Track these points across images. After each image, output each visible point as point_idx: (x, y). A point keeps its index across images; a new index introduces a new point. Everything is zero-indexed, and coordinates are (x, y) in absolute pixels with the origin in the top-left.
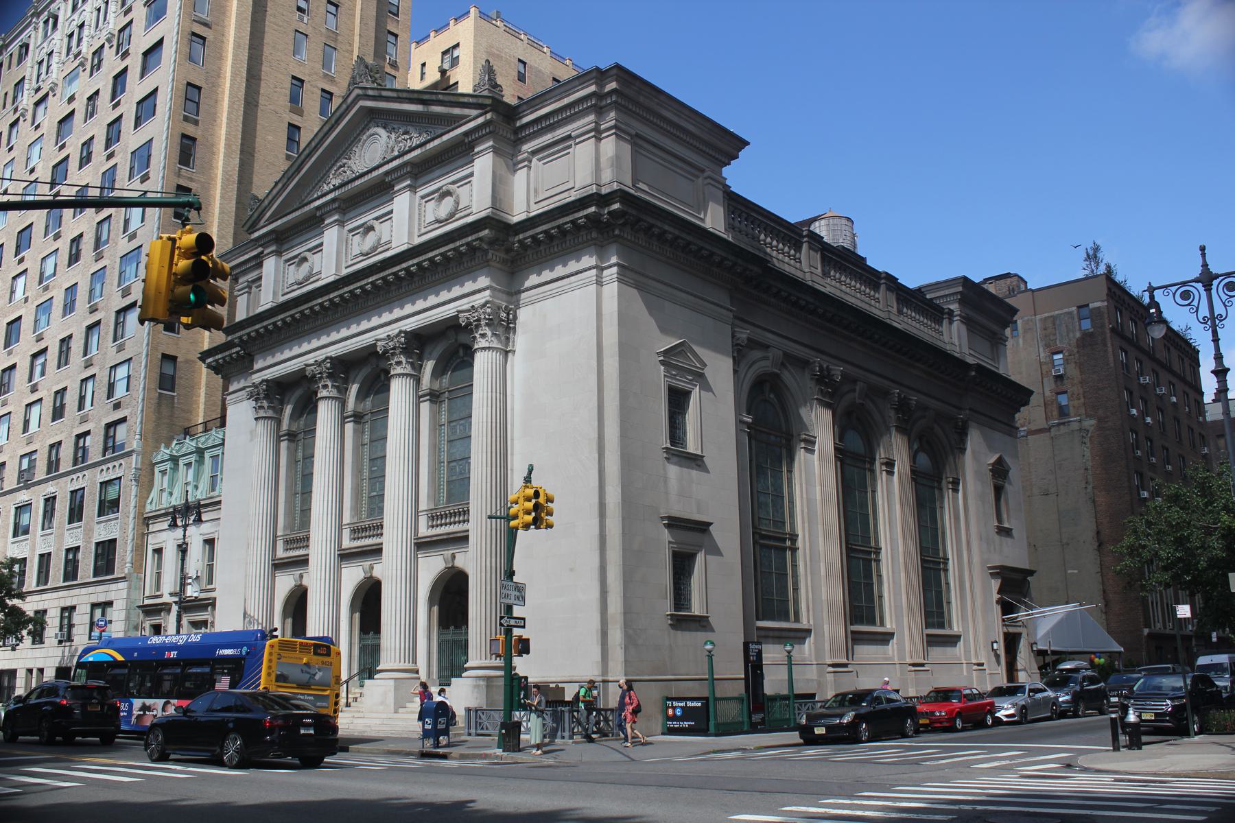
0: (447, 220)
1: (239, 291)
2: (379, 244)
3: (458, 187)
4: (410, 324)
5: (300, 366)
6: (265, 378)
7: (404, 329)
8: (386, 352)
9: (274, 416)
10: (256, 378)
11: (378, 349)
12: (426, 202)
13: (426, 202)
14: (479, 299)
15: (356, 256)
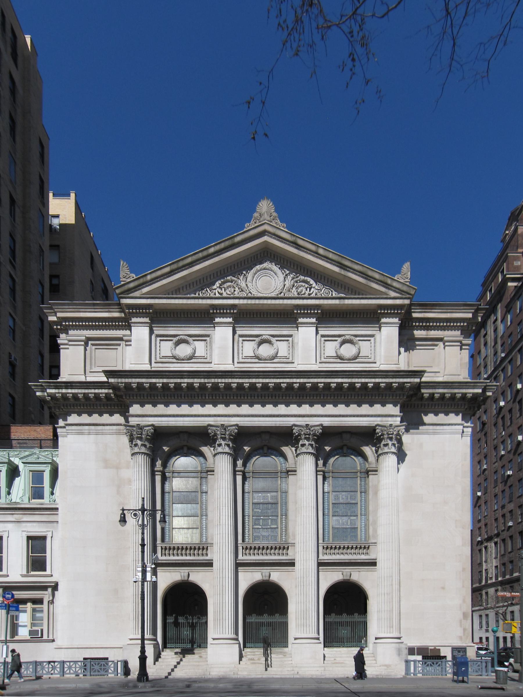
0: (349, 360)
1: (70, 341)
2: (277, 356)
3: (359, 340)
4: (327, 422)
5: (206, 424)
6: (154, 423)
7: (323, 423)
8: (300, 435)
9: (146, 452)
10: (133, 421)
11: (294, 431)
12: (325, 340)
13: (325, 340)
14: (390, 421)
15: (247, 357)
